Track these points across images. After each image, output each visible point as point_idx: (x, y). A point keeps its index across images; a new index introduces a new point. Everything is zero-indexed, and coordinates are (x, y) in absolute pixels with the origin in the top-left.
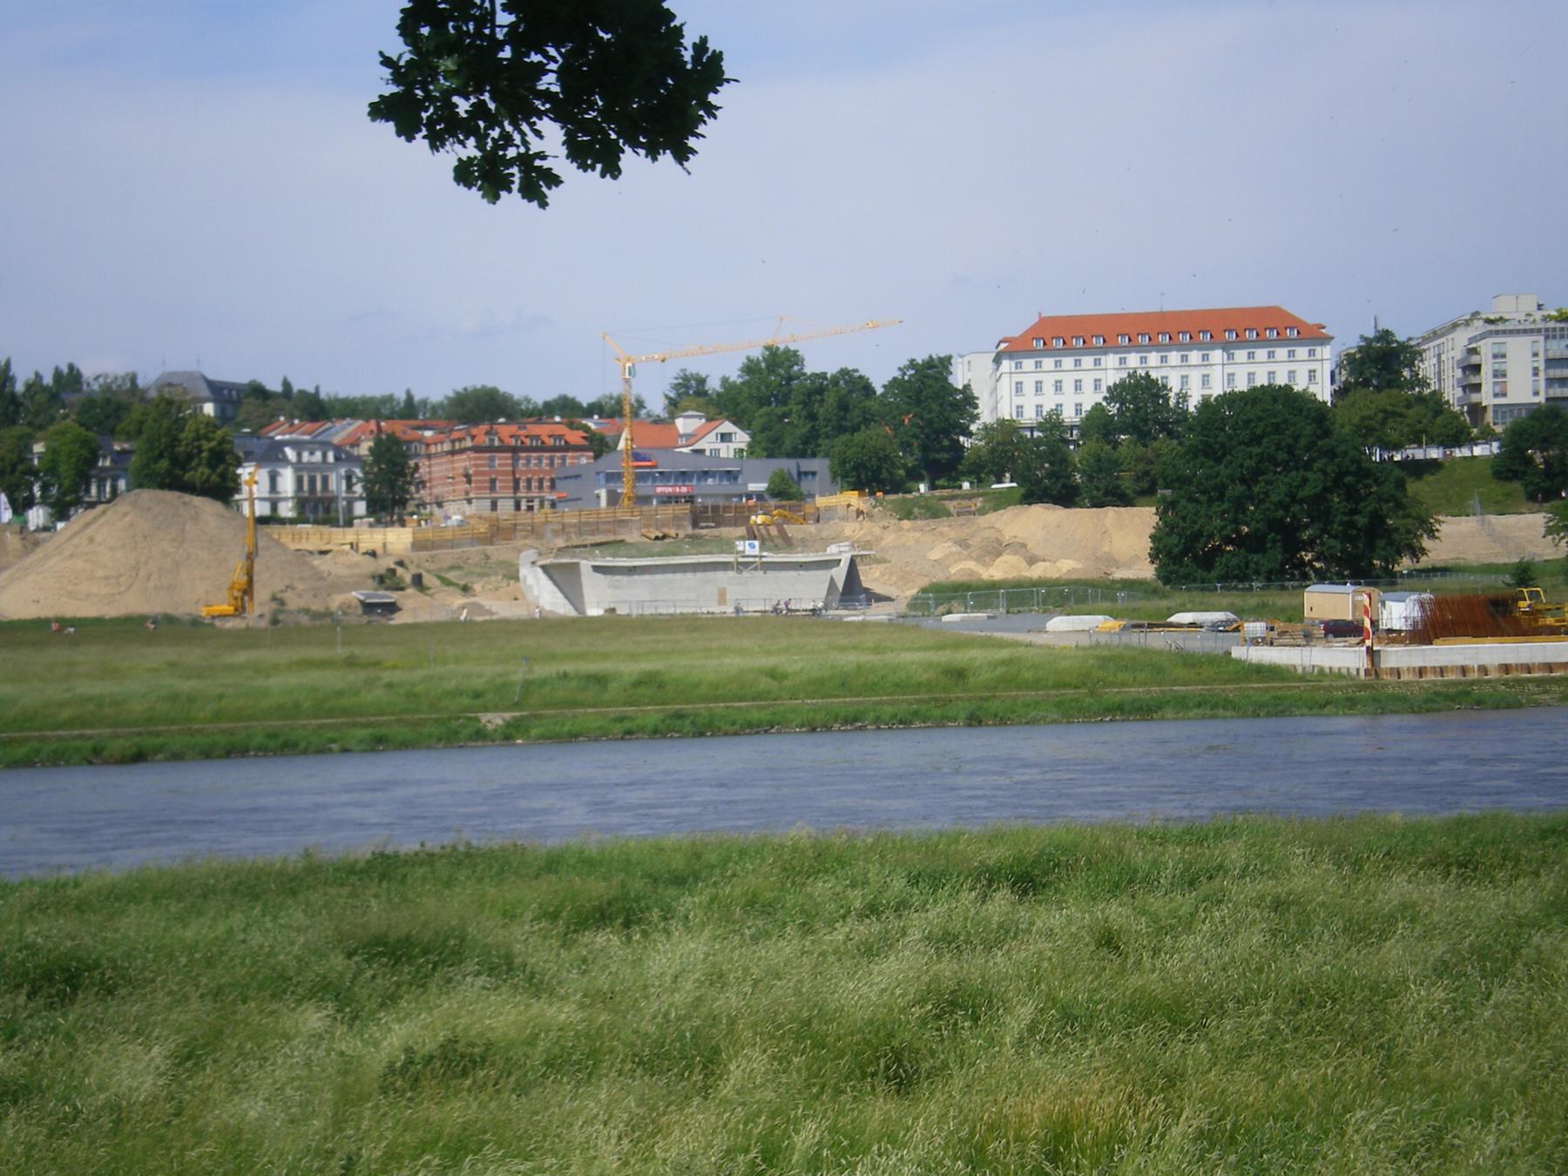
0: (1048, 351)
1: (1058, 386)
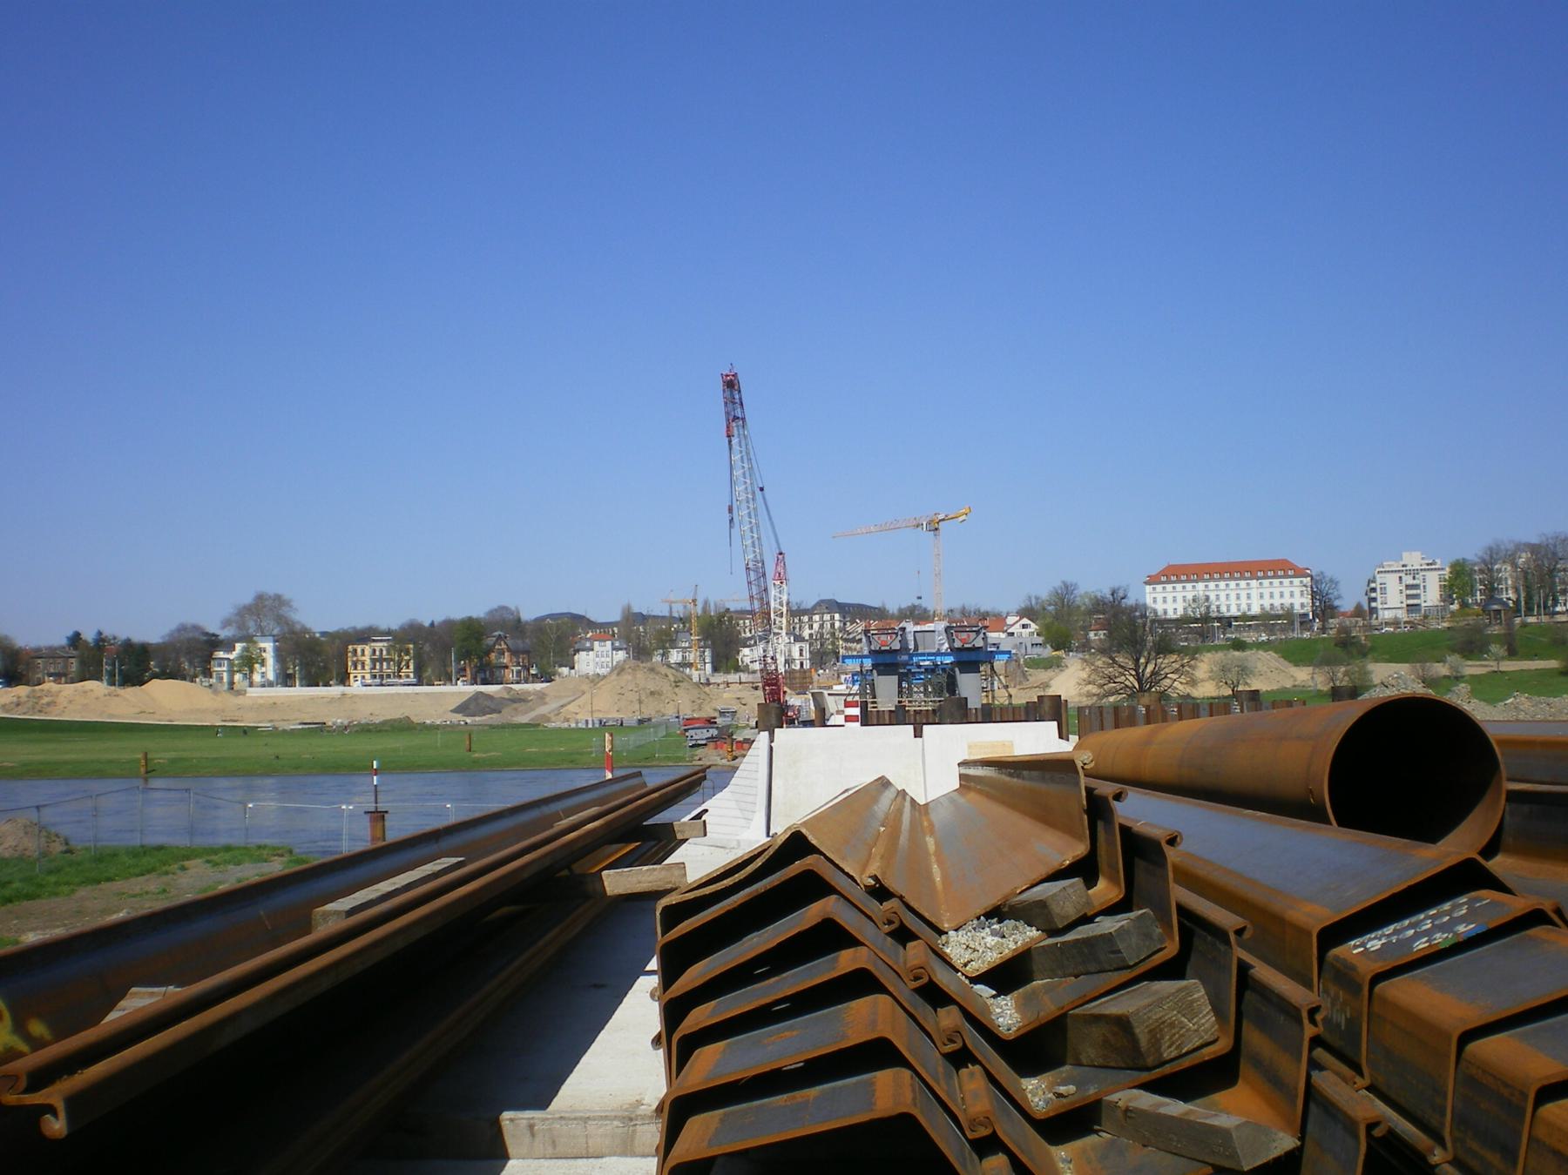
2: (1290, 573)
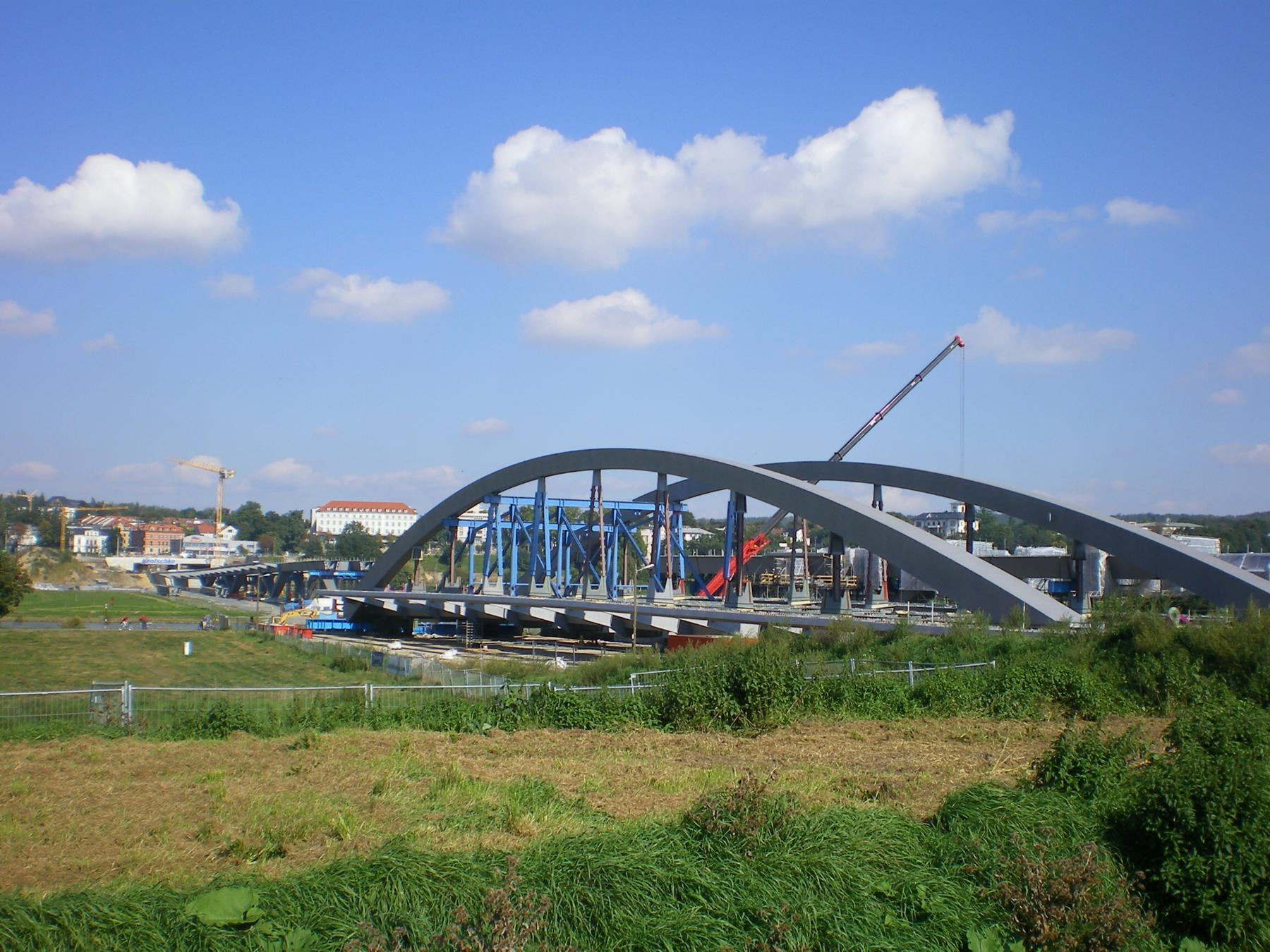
0: (332, 510)
1: (334, 523)
2: (406, 511)
